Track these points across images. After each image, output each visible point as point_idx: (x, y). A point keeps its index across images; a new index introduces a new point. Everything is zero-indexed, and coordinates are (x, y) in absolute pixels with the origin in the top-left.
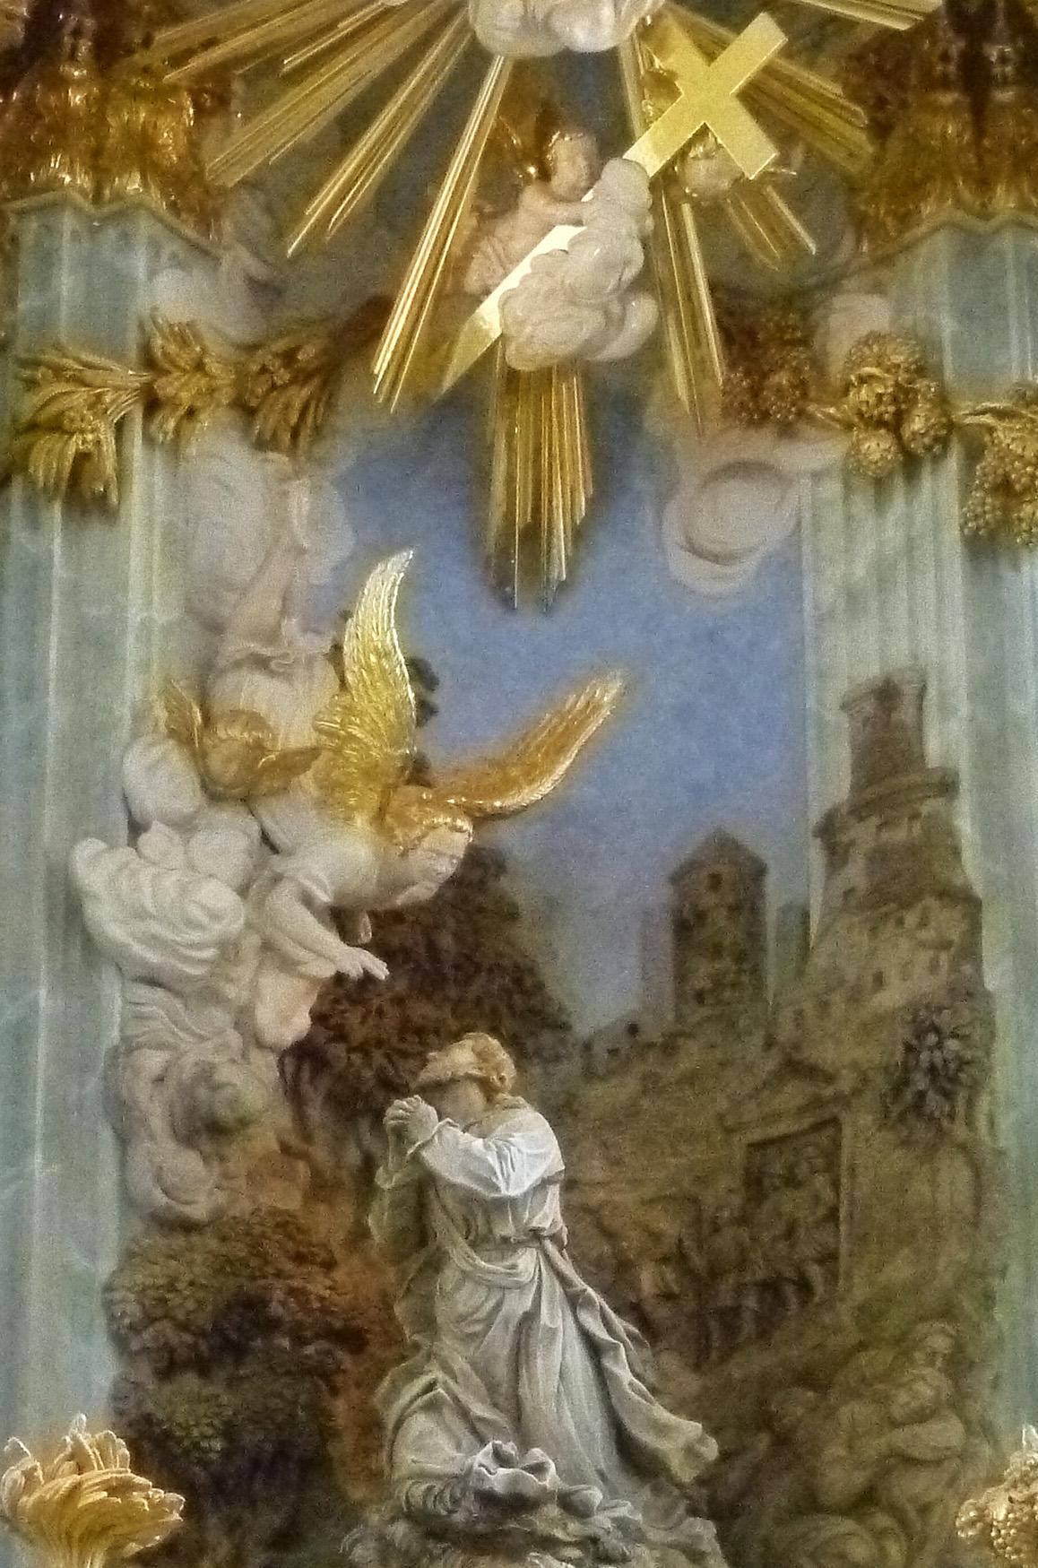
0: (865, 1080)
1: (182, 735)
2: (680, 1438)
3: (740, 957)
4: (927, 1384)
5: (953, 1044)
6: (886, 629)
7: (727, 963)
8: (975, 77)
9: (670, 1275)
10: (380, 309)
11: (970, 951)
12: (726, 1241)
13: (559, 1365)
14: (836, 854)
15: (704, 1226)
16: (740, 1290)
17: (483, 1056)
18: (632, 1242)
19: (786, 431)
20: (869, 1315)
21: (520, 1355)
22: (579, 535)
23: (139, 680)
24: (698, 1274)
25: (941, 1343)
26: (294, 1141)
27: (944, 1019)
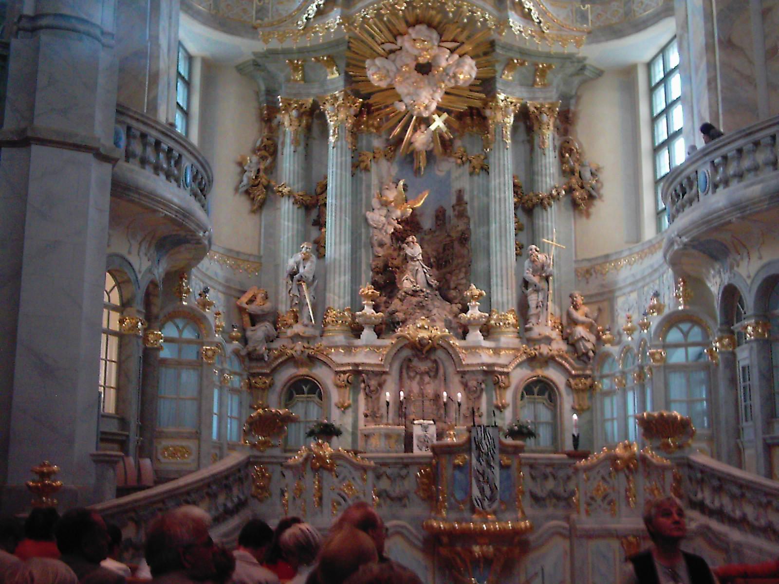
1: (378, 198)
4: (462, 275)
8: (472, 115)
10: (402, 140)
11: (468, 224)
13: (421, 275)
19: (450, 156)
20: (456, 266)
21: (417, 273)
22: (425, 168)
23: (375, 191)
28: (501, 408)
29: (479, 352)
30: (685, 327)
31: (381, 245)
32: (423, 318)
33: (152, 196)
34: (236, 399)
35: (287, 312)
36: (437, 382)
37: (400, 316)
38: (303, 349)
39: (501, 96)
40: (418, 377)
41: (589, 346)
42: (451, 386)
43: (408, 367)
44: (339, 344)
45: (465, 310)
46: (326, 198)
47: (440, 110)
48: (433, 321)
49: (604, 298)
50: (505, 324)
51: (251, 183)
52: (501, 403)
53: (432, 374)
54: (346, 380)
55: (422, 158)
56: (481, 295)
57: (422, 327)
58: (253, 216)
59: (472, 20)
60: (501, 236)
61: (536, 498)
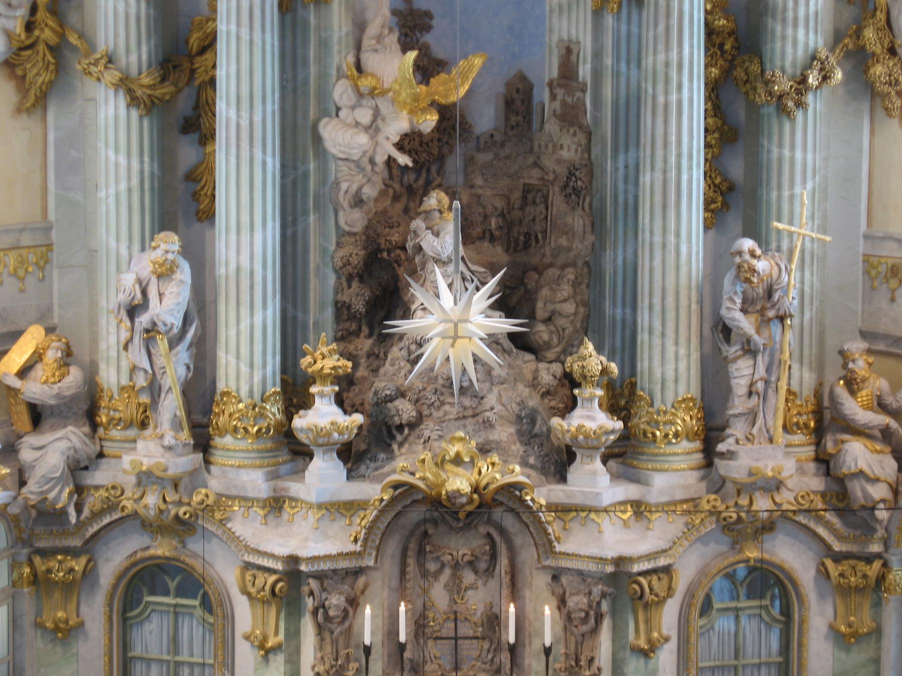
0: (556, 178)
3: (524, 117)
5: (579, 183)
6: (569, 23)
7: (520, 118)
9: (500, 220)
11: (588, 149)
12: (517, 214)
14: (553, 97)
15: (510, 207)
16: (519, 233)
17: (439, 202)
18: (490, 209)
24: (509, 225)
25: (571, 277)
26: (388, 182)
27: (577, 173)
31: (358, 201)
32: (461, 434)
35: (122, 389)
36: (493, 584)
37: (405, 410)
38: (163, 507)
40: (447, 572)
42: (527, 594)
43: (421, 553)
44: (251, 494)
46: (214, 66)
48: (488, 425)
50: (666, 436)
51: (17, 45)
52: (649, 641)
53: (483, 566)
54: (267, 588)
56: (605, 371)
57: (457, 460)
58: (24, 120)
60: (665, 206)
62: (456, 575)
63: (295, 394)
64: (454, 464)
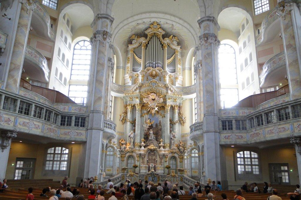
2: (155, 138)
4: (160, 137)
13: (152, 136)
23: (144, 121)
28: (166, 162)
29: (163, 151)
30: (195, 150)
31: (145, 131)
33: (108, 133)
34: (119, 159)
37: (149, 144)
39: (167, 104)
41: (182, 150)
45: (160, 143)
47: (156, 106)
49: (185, 142)
55: (154, 114)
57: (152, 147)
59: (162, 92)
61: (161, 180)
62: (152, 156)
63: (141, 143)
64: (152, 147)
